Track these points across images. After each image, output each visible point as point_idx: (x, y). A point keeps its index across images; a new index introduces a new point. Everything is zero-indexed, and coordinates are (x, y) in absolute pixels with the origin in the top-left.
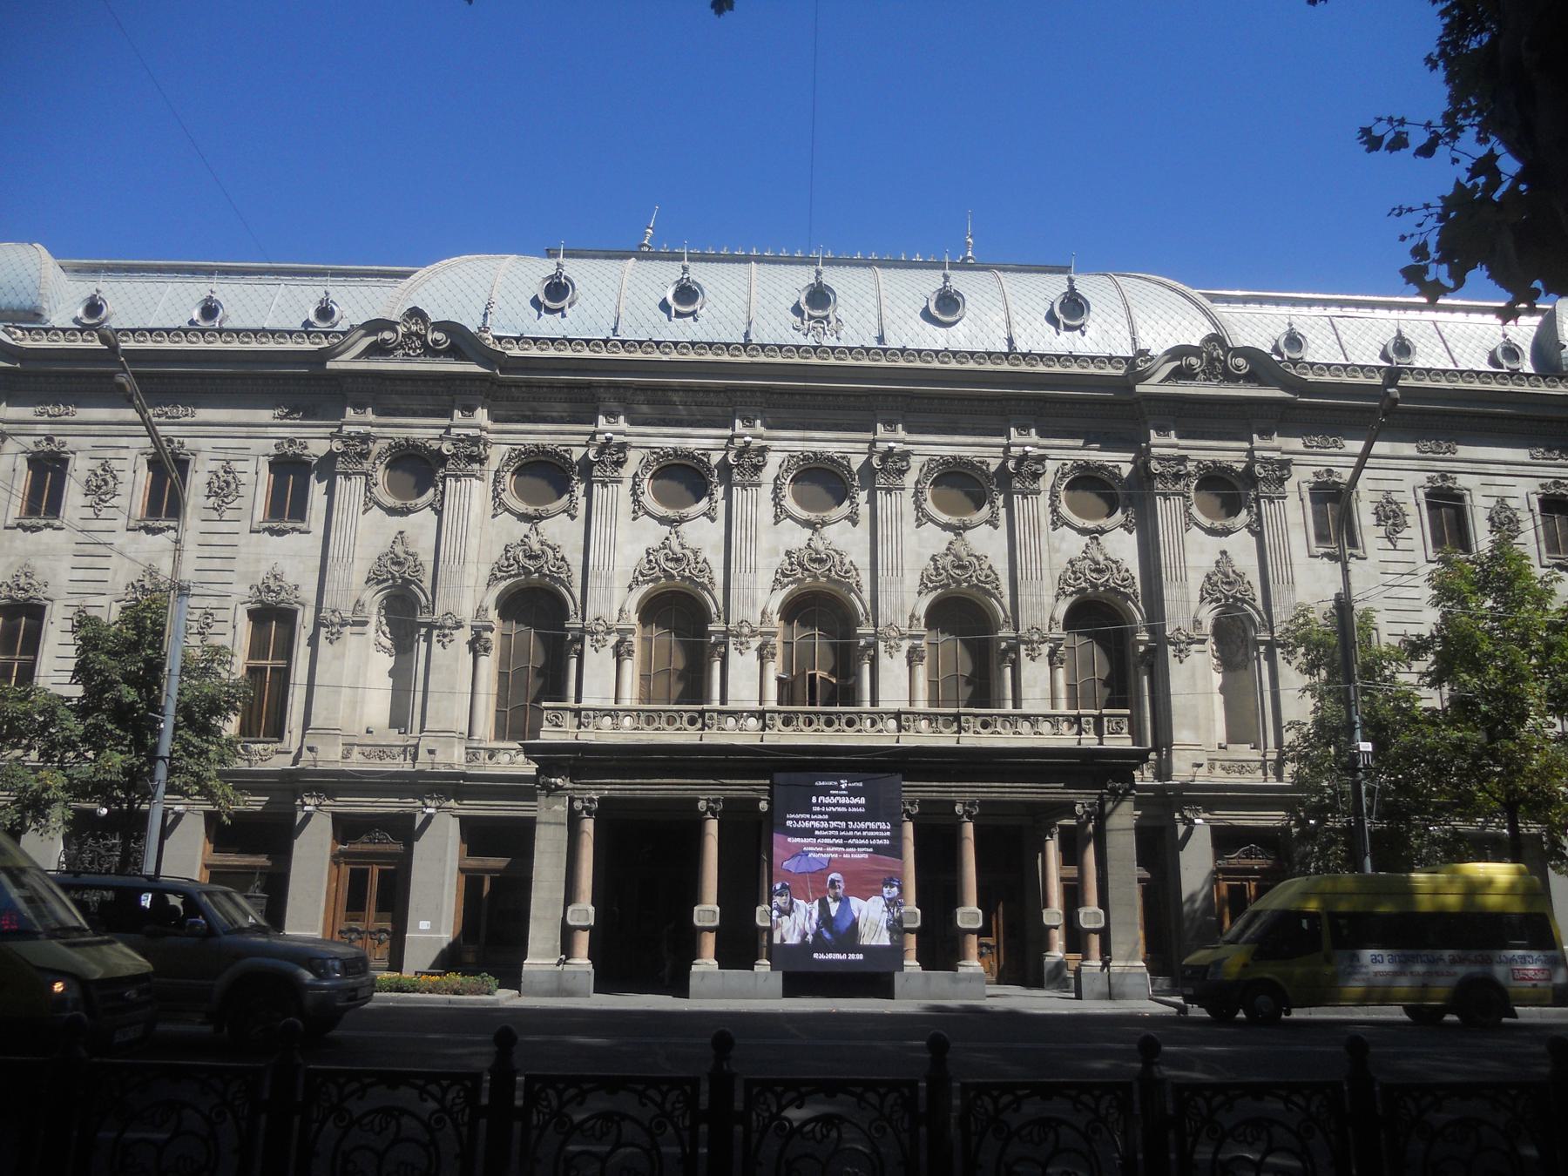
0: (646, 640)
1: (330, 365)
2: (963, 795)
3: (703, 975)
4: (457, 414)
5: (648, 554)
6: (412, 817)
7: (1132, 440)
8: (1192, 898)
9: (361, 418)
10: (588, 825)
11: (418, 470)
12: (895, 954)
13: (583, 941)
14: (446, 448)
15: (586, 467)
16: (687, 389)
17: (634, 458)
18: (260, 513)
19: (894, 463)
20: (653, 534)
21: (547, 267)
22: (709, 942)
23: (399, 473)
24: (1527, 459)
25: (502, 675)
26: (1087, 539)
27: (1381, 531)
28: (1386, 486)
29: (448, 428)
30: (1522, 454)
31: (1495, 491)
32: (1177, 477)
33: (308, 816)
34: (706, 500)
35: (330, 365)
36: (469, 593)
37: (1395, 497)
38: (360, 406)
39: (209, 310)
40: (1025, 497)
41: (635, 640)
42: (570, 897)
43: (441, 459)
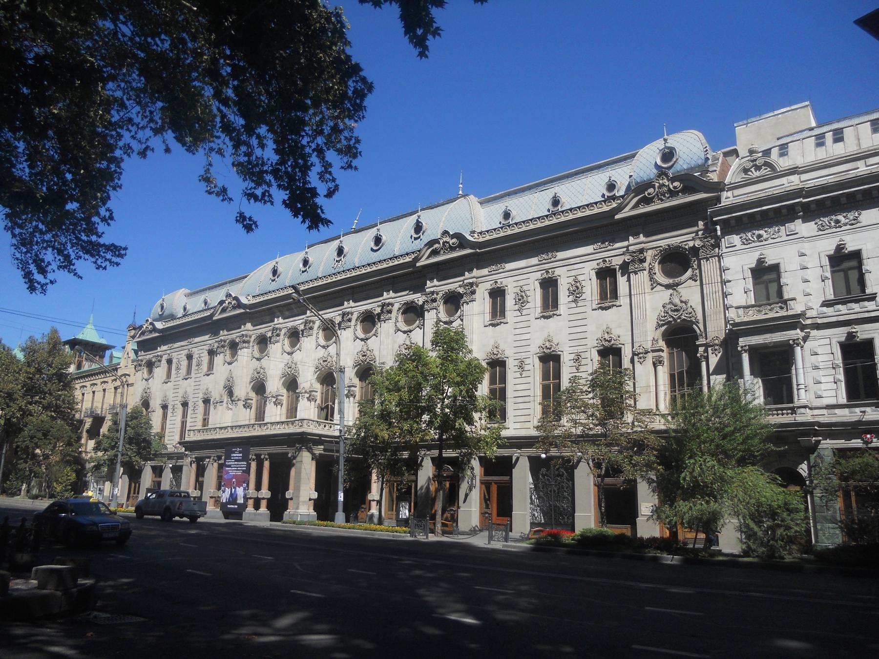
0: (671, 355)
1: (418, 264)
2: (265, 451)
3: (250, 513)
4: (466, 273)
5: (664, 307)
6: (511, 457)
7: (419, 288)
8: (421, 488)
9: (432, 284)
10: (267, 464)
11: (369, 320)
12: (244, 506)
13: (264, 503)
14: (461, 290)
15: (379, 315)
16: (277, 306)
17: (649, 255)
18: (539, 310)
19: (639, 257)
20: (664, 295)
21: (301, 255)
22: (340, 507)
23: (449, 305)
24: (537, 262)
25: (672, 376)
26: (671, 291)
27: (517, 307)
28: (521, 283)
29: (627, 247)
30: (589, 249)
31: (573, 273)
32: (434, 300)
33: (518, 459)
34: (690, 270)
35: (418, 264)
36: (308, 379)
37: (525, 288)
38: (431, 280)
39: (206, 303)
40: (707, 259)
41: (665, 355)
42: (258, 487)
43: (461, 296)
